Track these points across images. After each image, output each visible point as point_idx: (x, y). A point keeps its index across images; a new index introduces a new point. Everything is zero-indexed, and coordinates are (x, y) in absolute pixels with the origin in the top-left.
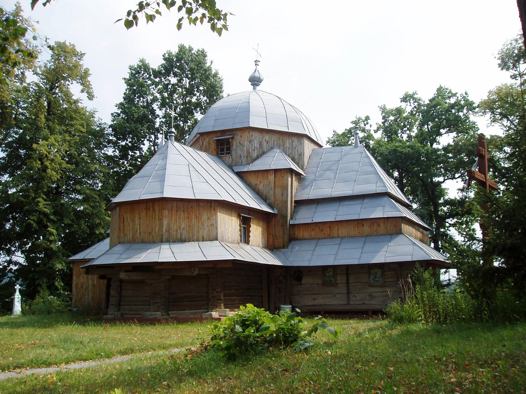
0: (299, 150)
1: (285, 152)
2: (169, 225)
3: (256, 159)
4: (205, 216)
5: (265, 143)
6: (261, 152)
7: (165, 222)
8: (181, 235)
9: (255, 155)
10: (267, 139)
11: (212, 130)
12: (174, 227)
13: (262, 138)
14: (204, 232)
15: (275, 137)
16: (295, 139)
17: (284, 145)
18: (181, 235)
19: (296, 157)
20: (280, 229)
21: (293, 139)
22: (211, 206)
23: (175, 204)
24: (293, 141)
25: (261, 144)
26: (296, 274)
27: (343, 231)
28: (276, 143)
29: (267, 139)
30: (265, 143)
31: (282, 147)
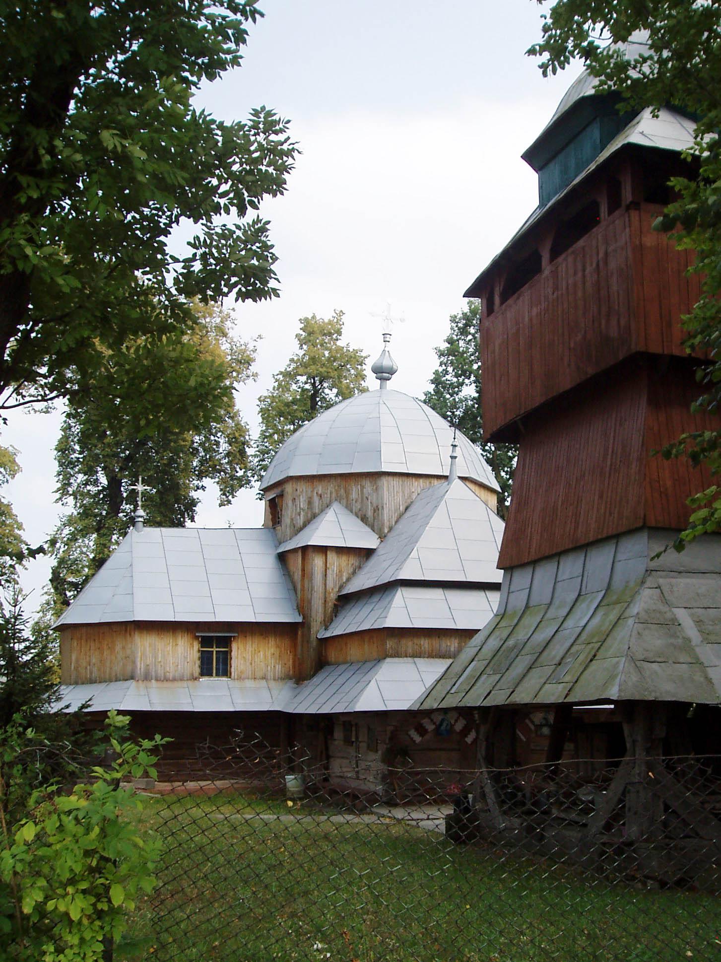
0: (374, 501)
1: (349, 507)
2: (77, 661)
3: (301, 529)
4: (118, 647)
5: (316, 499)
6: (309, 515)
7: (74, 657)
8: (91, 673)
9: (300, 521)
10: (320, 492)
11: (315, 473)
12: (84, 663)
13: (312, 491)
14: (117, 669)
15: (329, 489)
16: (368, 485)
17: (347, 497)
18: (91, 673)
19: (370, 514)
20: (308, 648)
21: (364, 482)
22: (126, 631)
23: (84, 630)
24: (363, 487)
25: (310, 503)
26: (324, 724)
27: (408, 644)
28: (334, 495)
29: (320, 492)
30: (316, 499)
31: (345, 501)
